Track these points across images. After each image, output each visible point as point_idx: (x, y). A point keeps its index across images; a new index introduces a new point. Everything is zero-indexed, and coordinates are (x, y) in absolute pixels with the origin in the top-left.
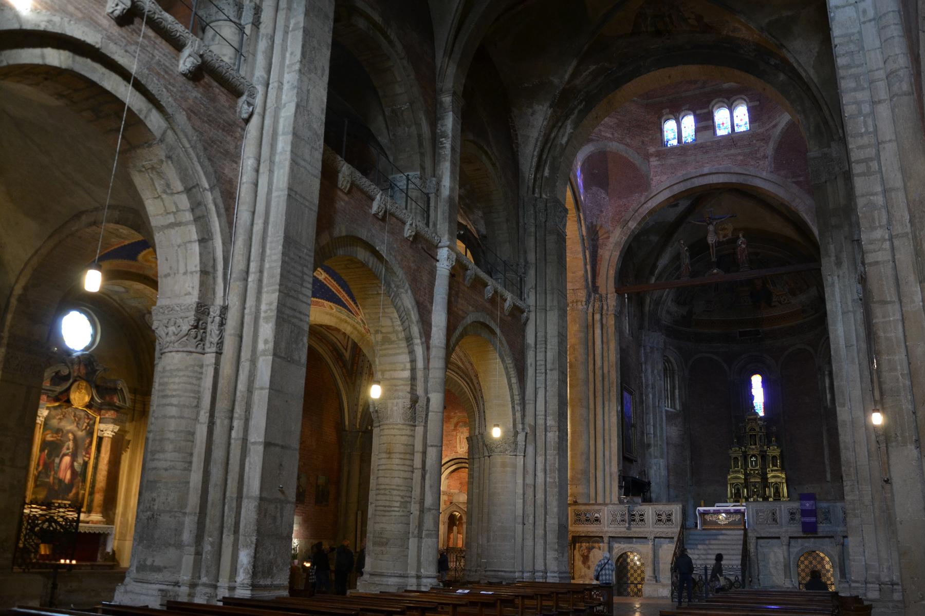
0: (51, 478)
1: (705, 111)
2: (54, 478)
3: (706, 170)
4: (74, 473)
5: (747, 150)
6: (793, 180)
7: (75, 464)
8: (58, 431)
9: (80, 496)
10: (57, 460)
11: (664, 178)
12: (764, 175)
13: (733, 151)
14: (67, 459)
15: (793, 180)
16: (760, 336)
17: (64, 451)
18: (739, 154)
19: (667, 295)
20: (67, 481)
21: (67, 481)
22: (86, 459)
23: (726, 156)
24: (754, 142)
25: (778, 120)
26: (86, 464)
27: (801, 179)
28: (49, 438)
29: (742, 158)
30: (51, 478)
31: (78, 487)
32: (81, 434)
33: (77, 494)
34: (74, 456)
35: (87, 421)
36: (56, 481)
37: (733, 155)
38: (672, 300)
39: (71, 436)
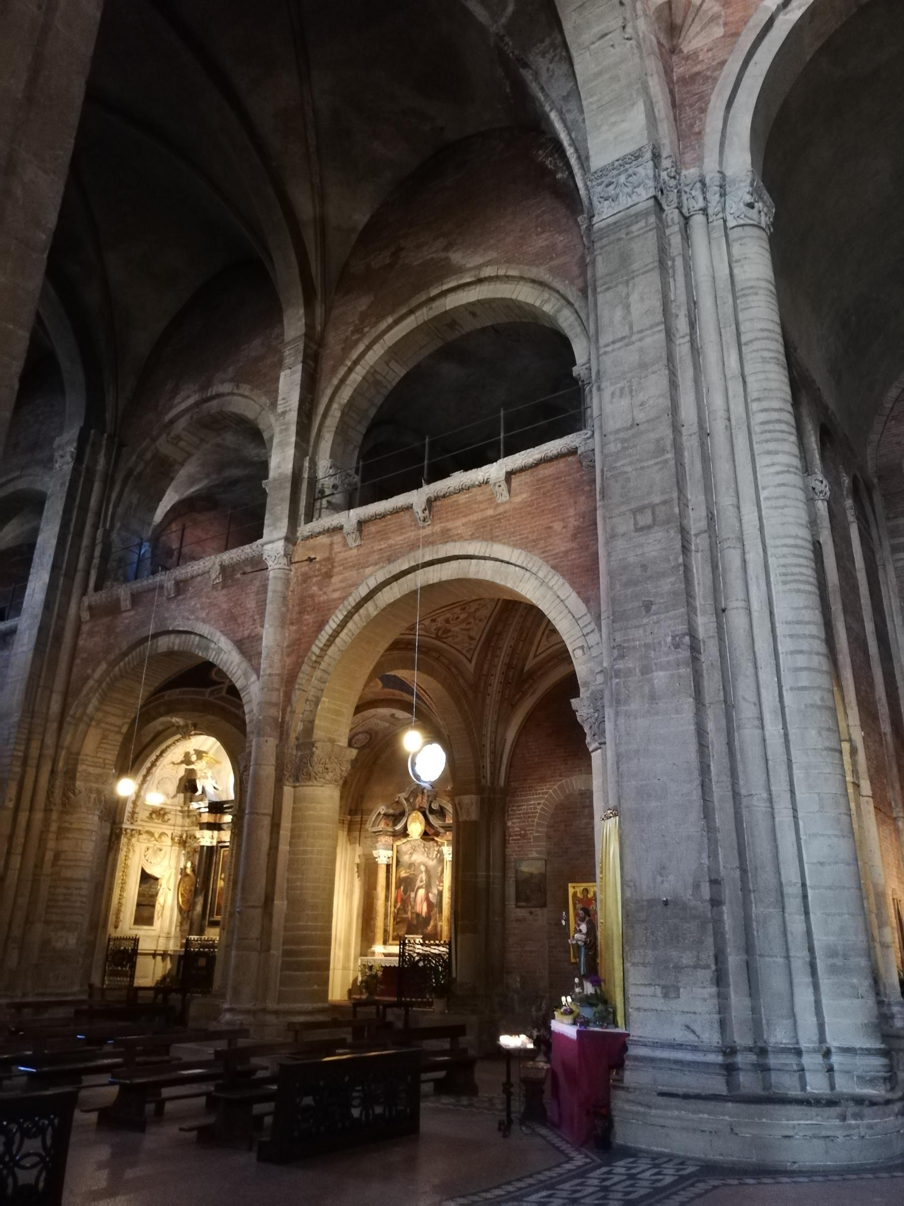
0: (409, 913)
2: (412, 913)
4: (430, 905)
7: (430, 895)
8: (411, 865)
9: (439, 929)
10: (413, 895)
14: (422, 892)
17: (418, 884)
20: (424, 914)
21: (424, 914)
22: (440, 888)
26: (440, 894)
28: (403, 874)
30: (409, 913)
31: (436, 919)
32: (432, 863)
33: (435, 926)
34: (428, 887)
35: (436, 849)
36: (414, 916)
39: (423, 868)
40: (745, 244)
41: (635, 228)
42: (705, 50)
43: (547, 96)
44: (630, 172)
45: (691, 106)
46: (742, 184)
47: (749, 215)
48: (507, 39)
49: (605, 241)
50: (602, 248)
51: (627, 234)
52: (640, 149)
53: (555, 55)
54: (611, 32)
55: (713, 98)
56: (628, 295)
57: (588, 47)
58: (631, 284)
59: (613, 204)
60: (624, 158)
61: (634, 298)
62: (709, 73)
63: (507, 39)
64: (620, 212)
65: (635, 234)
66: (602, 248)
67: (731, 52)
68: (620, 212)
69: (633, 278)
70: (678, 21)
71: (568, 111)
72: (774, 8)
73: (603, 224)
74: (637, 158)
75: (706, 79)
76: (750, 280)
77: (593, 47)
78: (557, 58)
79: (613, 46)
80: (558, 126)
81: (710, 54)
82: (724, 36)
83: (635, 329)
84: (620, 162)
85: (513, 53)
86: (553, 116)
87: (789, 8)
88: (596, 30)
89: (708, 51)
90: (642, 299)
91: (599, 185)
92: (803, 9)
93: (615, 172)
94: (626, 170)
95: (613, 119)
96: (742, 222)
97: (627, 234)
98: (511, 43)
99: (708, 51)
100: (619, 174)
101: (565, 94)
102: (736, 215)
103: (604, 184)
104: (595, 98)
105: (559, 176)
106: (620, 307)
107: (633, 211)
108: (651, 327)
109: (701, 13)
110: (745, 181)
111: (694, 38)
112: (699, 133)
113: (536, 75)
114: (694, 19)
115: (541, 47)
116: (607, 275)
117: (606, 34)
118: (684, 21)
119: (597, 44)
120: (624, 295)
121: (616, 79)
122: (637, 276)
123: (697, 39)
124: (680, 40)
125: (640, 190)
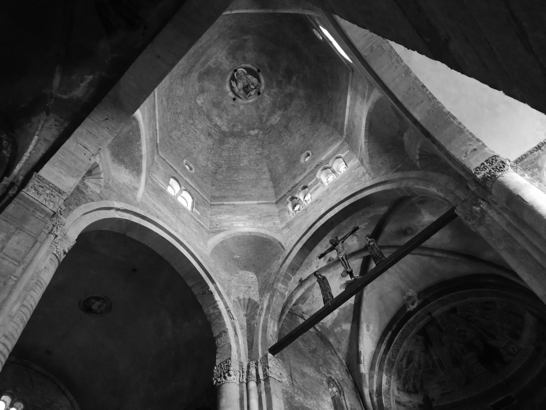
1: (314, 180)
3: (323, 212)
5: (350, 180)
6: (394, 171)
11: (294, 236)
12: (368, 184)
13: (339, 187)
15: (394, 171)
16: (516, 402)
18: (345, 185)
19: (389, 382)
23: (336, 193)
24: (353, 171)
25: (361, 143)
27: (399, 166)
29: (347, 186)
37: (341, 189)
38: (398, 389)
40: (52, 264)
41: (38, 213)
42: (91, 190)
43: (41, 130)
44: (53, 193)
45: (74, 199)
46: (68, 243)
47: (61, 255)
48: (53, 100)
49: (21, 202)
50: (18, 203)
51: (33, 211)
52: (64, 192)
53: (59, 127)
54: (88, 150)
55: (83, 206)
56: (14, 233)
57: (78, 143)
58: (18, 231)
59: (36, 194)
60: (56, 187)
61: (15, 238)
62: (87, 197)
63: (53, 100)
64: (37, 201)
65: (36, 216)
66: (18, 203)
67: (97, 201)
68: (37, 201)
69: (21, 230)
70: (93, 173)
71: (41, 144)
72: (115, 207)
73: (26, 196)
74: (60, 193)
75: (84, 198)
76: (43, 280)
77: (79, 145)
78: (57, 127)
79: (85, 154)
80: (34, 142)
81: (91, 193)
82: (98, 194)
83: (4, 251)
84: (53, 186)
85: (49, 105)
86: (36, 137)
87: (117, 212)
88: (86, 143)
89: (91, 191)
90: (18, 243)
91: (38, 182)
92: (121, 218)
93: (47, 186)
94: (52, 191)
95: (62, 171)
96: (57, 255)
97: (33, 211)
98: (52, 102)
99: (91, 191)
100: (48, 189)
101: (47, 138)
102: (58, 251)
103: (40, 184)
104: (63, 157)
105: (4, 152)
106: (5, 234)
107: (43, 207)
108: (13, 259)
109: (99, 179)
110: (70, 243)
111: (91, 182)
112: (71, 210)
113: (46, 121)
114: (96, 178)
115: (58, 118)
116: (11, 215)
117: (86, 148)
118: (96, 174)
119: (81, 146)
120: (11, 231)
121: (76, 163)
122: (24, 231)
123: (91, 183)
124: (87, 177)
125: (51, 204)
